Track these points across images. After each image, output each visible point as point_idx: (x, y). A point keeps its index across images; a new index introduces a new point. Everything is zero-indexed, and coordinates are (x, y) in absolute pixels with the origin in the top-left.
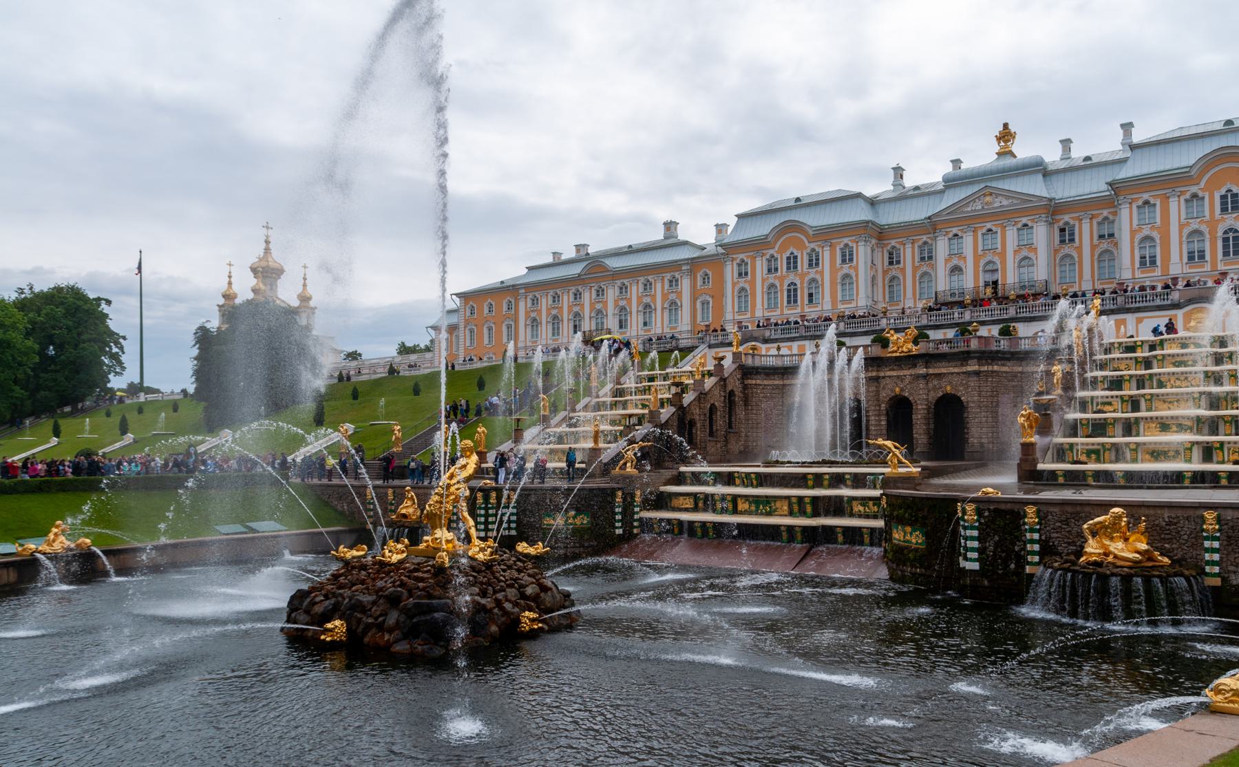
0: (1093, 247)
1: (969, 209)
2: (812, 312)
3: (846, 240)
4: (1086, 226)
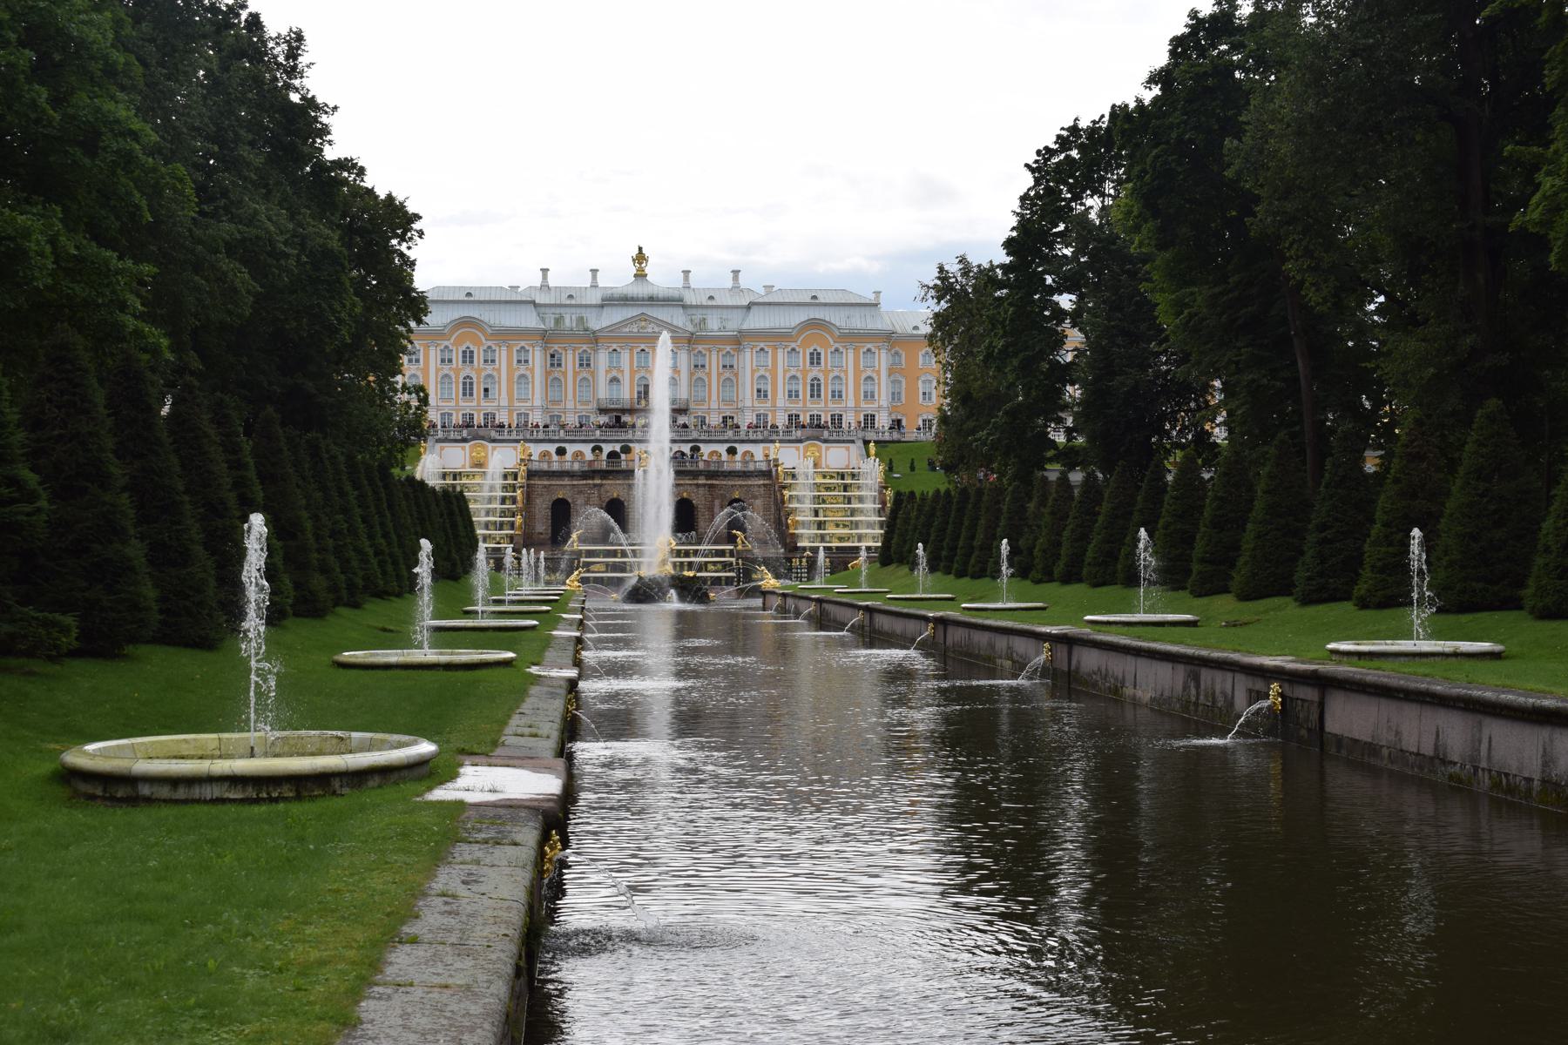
0: (719, 375)
1: (627, 330)
2: (488, 406)
3: (523, 343)
4: (714, 357)
